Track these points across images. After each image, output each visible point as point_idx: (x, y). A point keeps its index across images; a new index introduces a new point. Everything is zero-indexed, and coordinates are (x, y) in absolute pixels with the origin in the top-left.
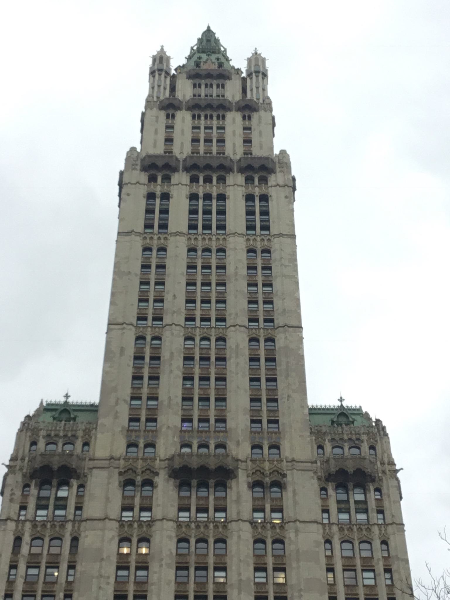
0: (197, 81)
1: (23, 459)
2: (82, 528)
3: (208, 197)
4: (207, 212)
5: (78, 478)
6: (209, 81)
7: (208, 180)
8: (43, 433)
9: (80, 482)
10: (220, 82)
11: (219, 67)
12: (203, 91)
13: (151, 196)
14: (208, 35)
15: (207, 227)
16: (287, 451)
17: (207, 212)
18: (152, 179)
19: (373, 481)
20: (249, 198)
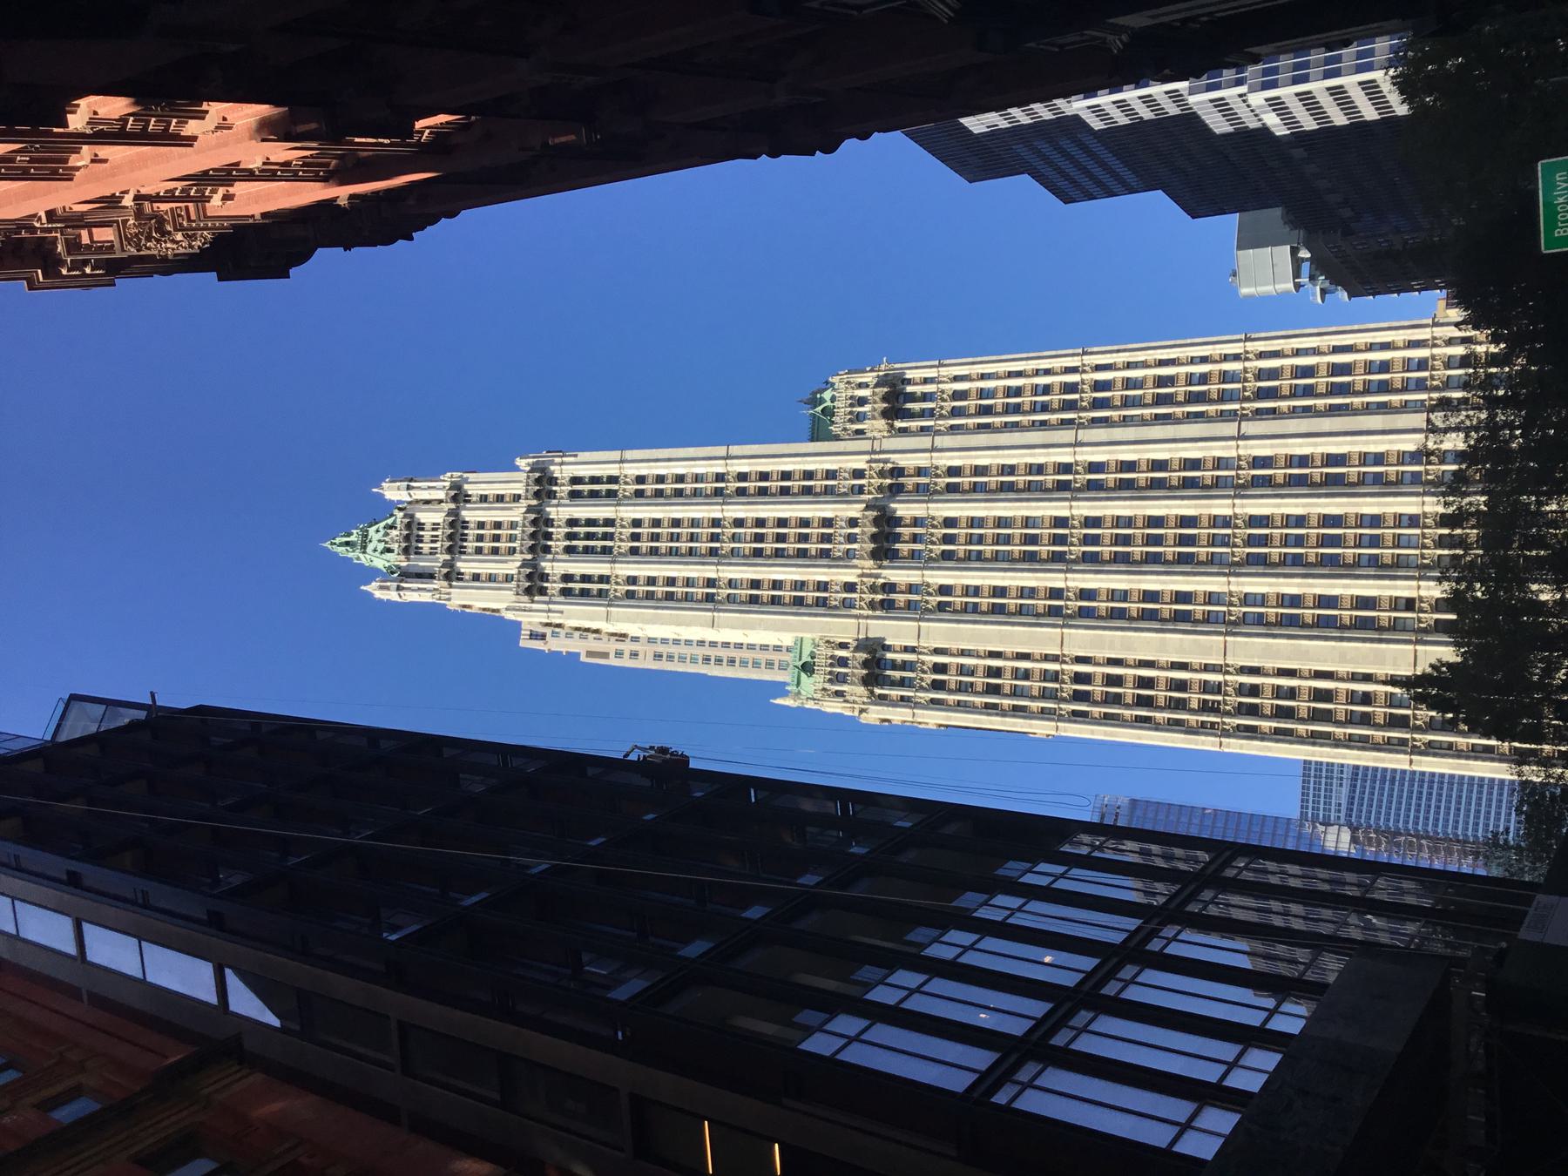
0: (412, 550)
1: (854, 702)
2: (926, 645)
3: (570, 536)
4: (589, 536)
5: (876, 650)
6: (413, 539)
7: (549, 536)
8: (828, 686)
9: (879, 649)
10: (414, 527)
11: (396, 528)
12: (426, 547)
13: (566, 592)
15: (606, 537)
16: (859, 463)
17: (589, 536)
18: (543, 591)
20: (574, 495)
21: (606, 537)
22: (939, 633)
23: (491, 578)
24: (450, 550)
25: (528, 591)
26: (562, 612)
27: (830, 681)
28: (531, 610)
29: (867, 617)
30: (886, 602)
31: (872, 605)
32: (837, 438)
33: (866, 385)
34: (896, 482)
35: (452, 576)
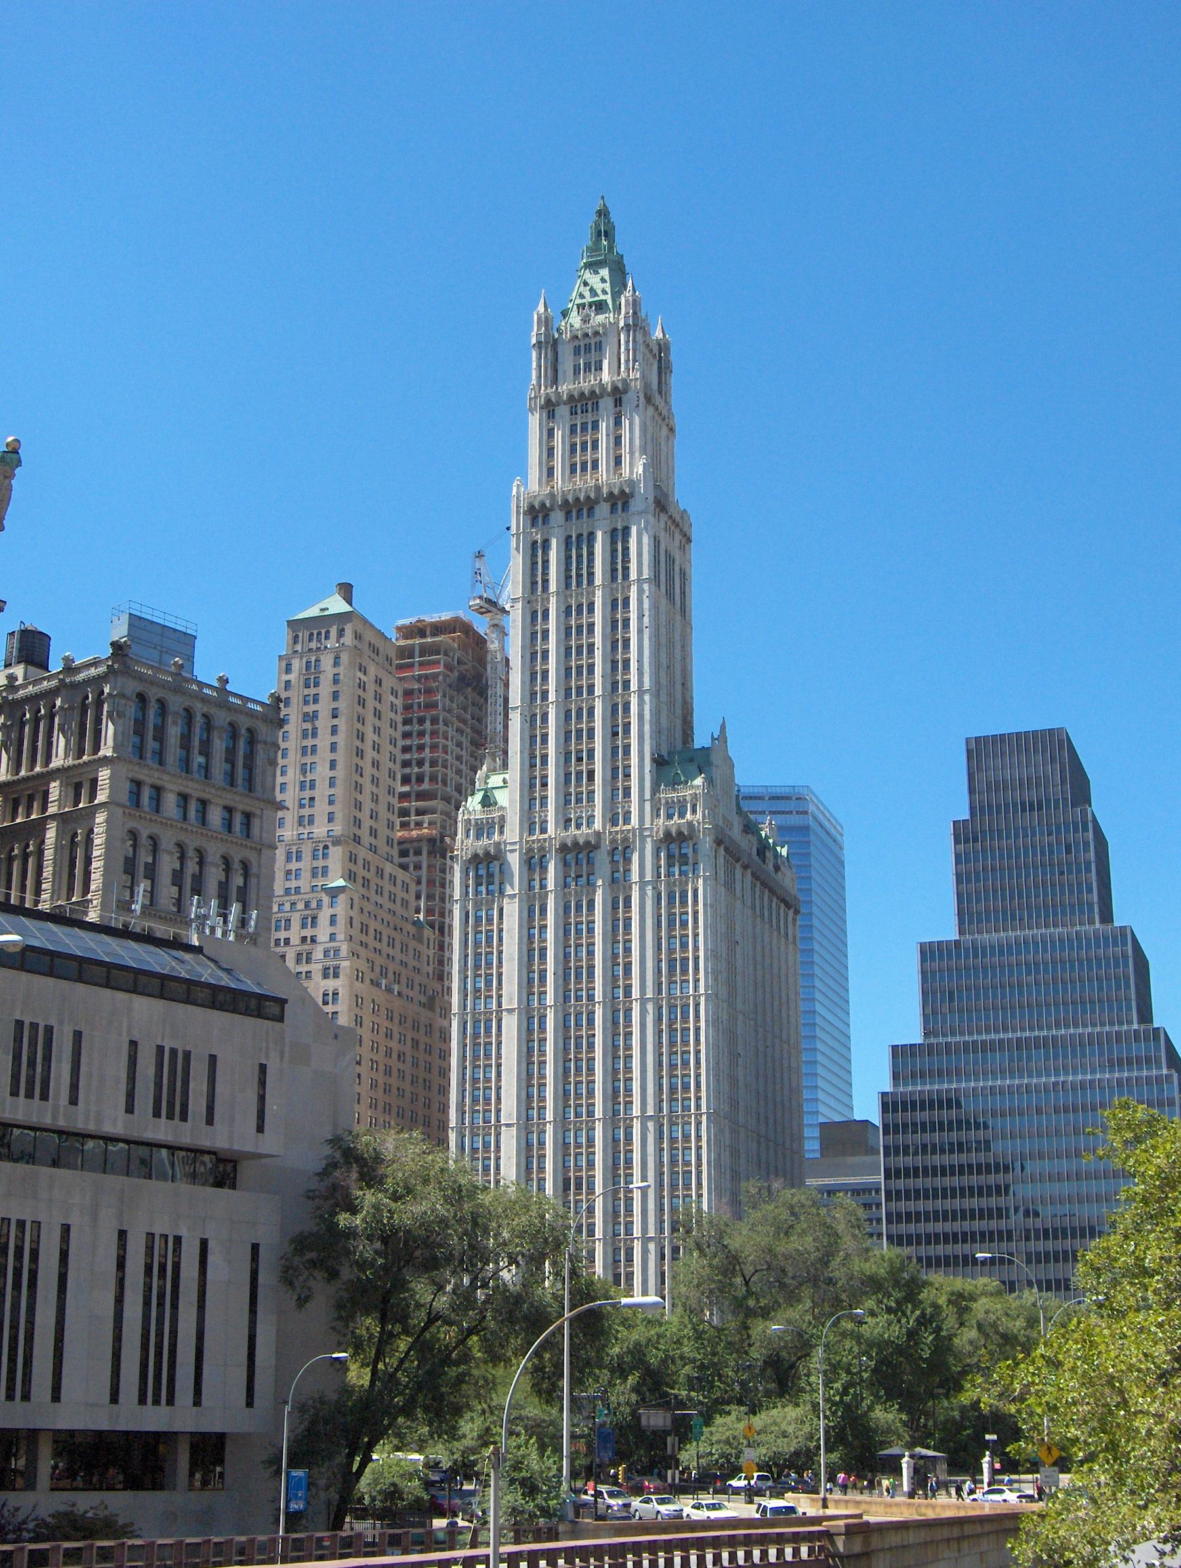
0: (576, 343)
14: (603, 213)
15: (579, 576)
19: (691, 838)
21: (579, 576)
22: (512, 911)
23: (551, 451)
24: (571, 397)
25: (531, 508)
26: (517, 549)
27: (477, 824)
28: (518, 513)
29: (521, 849)
30: (534, 862)
31: (530, 850)
32: (655, 790)
33: (694, 811)
34: (622, 851)
35: (550, 408)
